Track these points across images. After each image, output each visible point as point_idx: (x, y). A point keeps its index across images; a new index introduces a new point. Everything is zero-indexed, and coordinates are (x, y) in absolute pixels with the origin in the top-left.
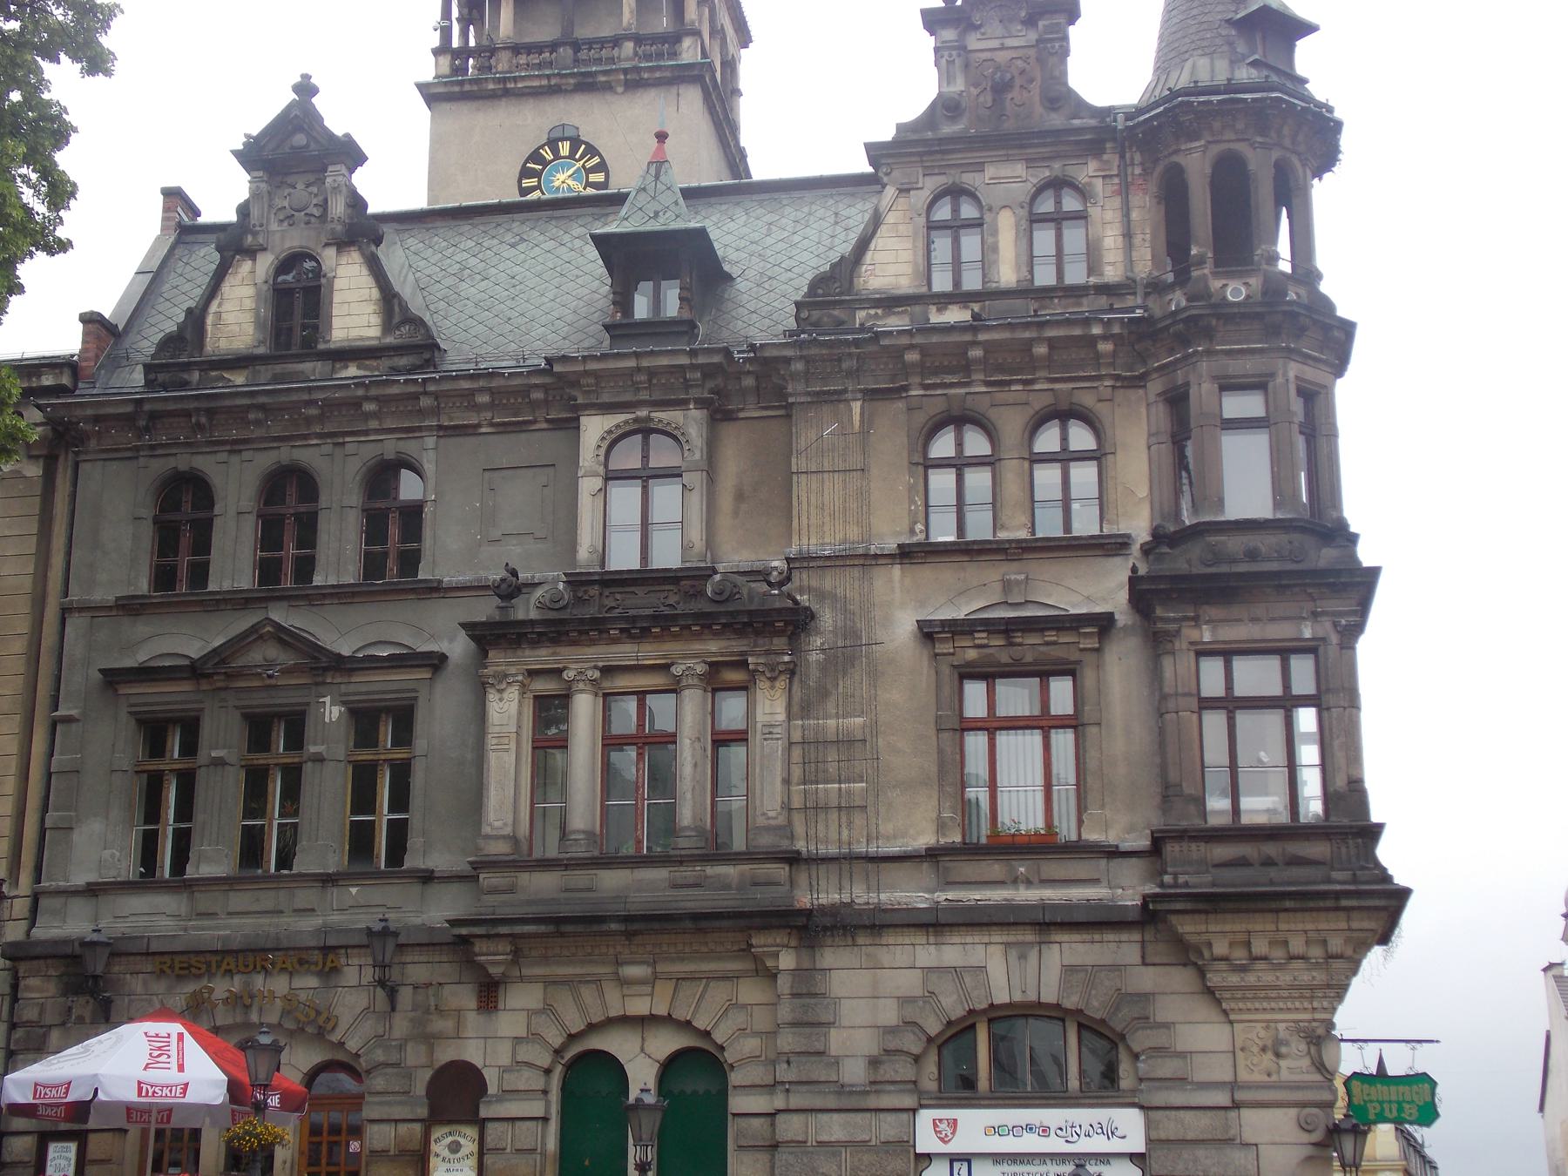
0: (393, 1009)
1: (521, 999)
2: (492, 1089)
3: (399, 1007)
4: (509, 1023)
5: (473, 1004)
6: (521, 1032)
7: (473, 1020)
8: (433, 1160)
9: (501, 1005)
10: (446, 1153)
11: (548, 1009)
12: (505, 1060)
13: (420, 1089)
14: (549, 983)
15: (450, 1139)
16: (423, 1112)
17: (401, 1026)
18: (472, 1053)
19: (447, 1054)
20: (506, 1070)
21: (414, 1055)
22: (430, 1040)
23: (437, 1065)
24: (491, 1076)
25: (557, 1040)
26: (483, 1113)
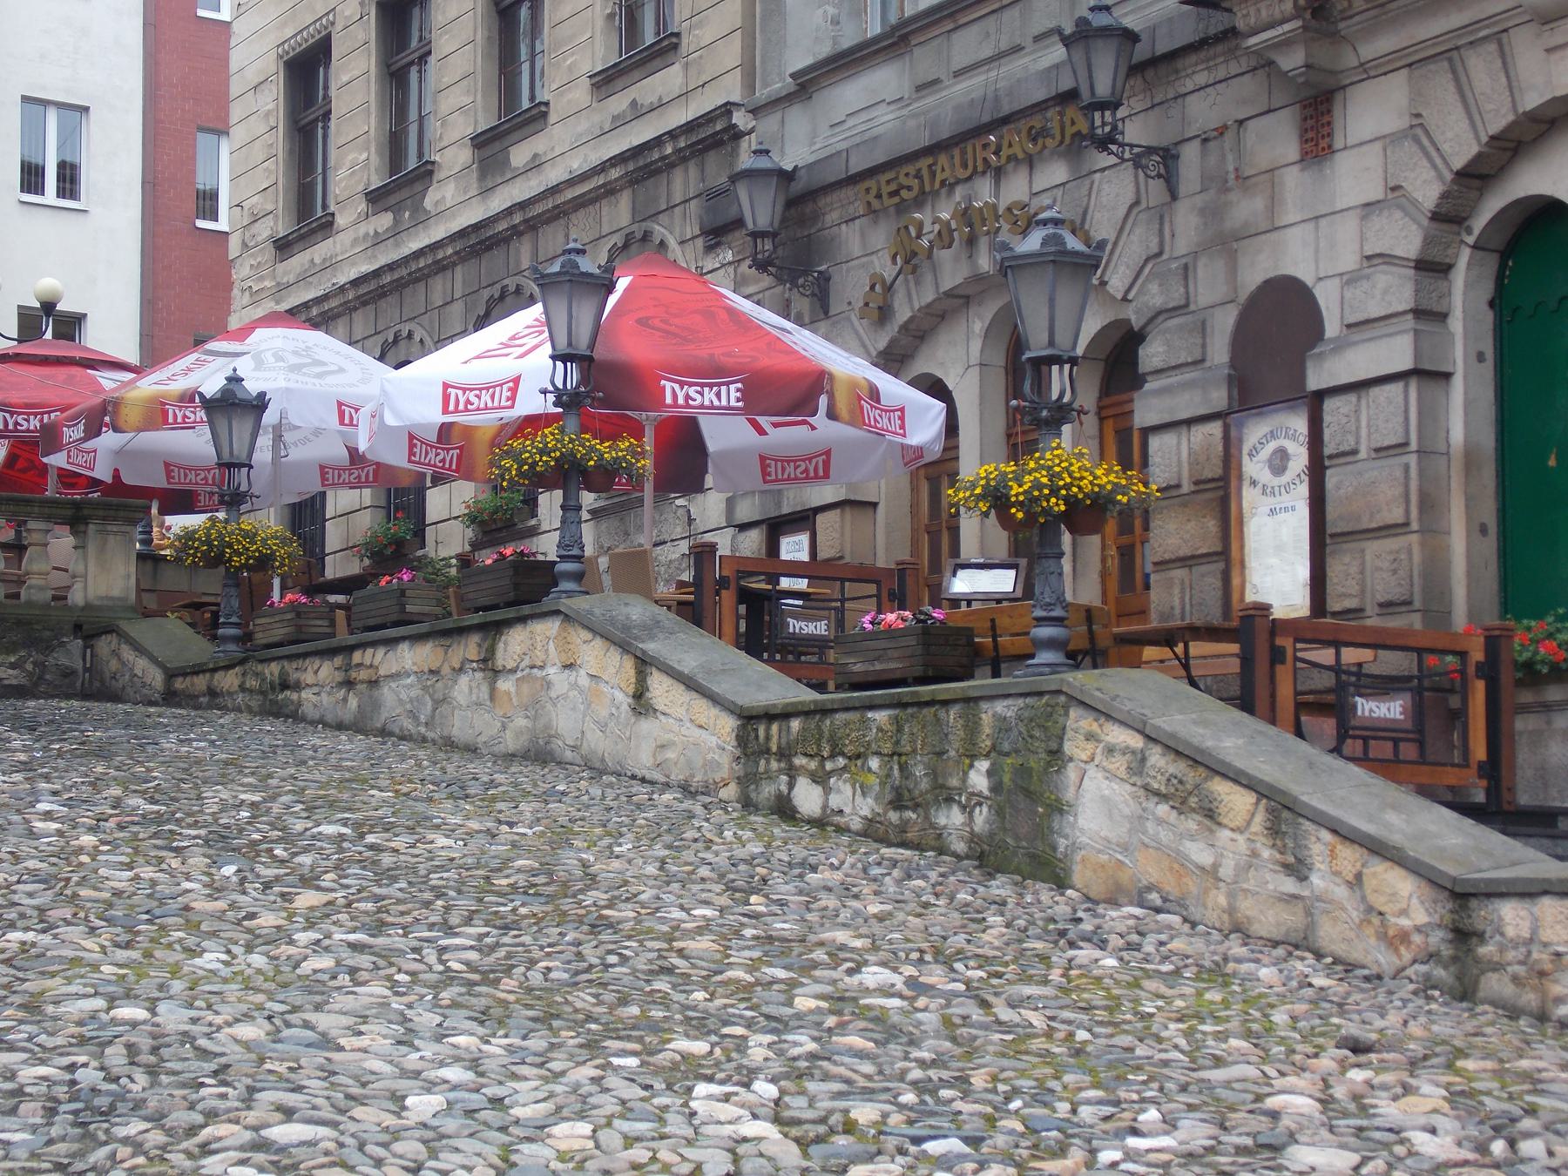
0: (1174, 197)
1: (1370, 114)
2: (1332, 329)
3: (1183, 190)
4: (1355, 176)
5: (1291, 151)
6: (1375, 192)
7: (1293, 179)
8: (1249, 495)
9: (1338, 143)
10: (1265, 476)
11: (1417, 130)
12: (1349, 261)
13: (1219, 353)
14: (1414, 62)
15: (1272, 446)
16: (1219, 398)
17: (1187, 225)
18: (1296, 256)
19: (1256, 271)
20: (1350, 279)
21: (1209, 286)
22: (1226, 243)
23: (1243, 296)
24: (1327, 298)
25: (1427, 190)
26: (1314, 382)
